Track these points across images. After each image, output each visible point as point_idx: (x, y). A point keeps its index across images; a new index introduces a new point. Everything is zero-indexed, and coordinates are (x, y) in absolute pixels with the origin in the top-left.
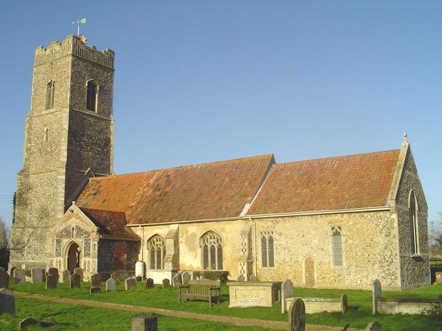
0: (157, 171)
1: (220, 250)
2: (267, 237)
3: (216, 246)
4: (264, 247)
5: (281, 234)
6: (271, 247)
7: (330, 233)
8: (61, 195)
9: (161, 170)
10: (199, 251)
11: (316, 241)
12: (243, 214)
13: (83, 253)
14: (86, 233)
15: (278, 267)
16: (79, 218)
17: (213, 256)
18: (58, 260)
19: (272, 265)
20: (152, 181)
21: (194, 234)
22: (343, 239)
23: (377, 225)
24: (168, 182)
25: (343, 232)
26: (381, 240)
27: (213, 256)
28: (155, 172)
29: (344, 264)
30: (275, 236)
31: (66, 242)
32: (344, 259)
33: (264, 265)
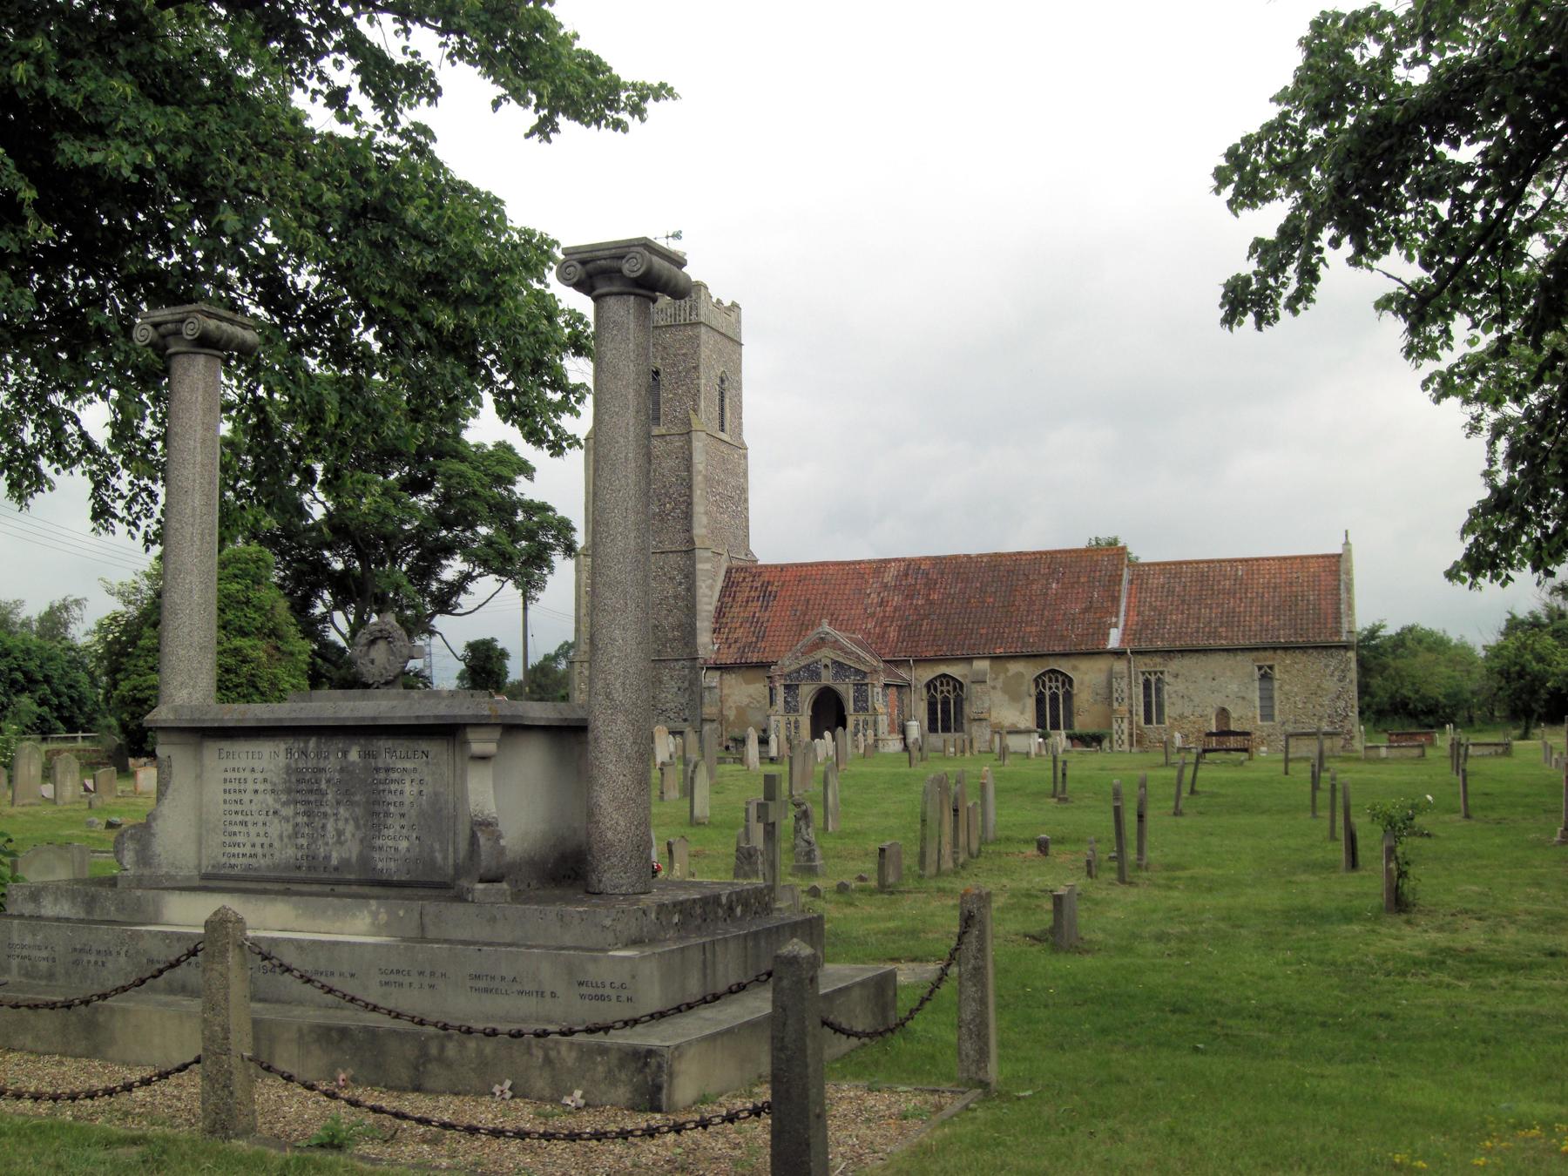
0: (895, 560)
1: (1069, 696)
2: (1153, 679)
3: (1061, 693)
4: (1147, 695)
5: (1176, 676)
6: (1159, 691)
7: (1257, 674)
8: (706, 600)
9: (904, 560)
10: (1031, 703)
11: (1234, 687)
12: (1114, 640)
13: (850, 706)
14: (857, 672)
15: (1172, 726)
16: (842, 649)
17: (1055, 708)
18: (792, 719)
19: (1159, 721)
20: (888, 578)
21: (1020, 675)
22: (1276, 684)
23: (1327, 666)
24: (931, 585)
25: (1277, 673)
26: (1331, 685)
27: (1055, 708)
28: (887, 561)
29: (1277, 718)
30: (1167, 678)
31: (807, 692)
32: (1277, 712)
33: (1148, 720)
